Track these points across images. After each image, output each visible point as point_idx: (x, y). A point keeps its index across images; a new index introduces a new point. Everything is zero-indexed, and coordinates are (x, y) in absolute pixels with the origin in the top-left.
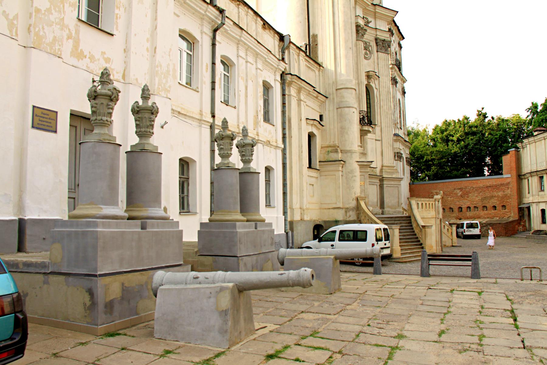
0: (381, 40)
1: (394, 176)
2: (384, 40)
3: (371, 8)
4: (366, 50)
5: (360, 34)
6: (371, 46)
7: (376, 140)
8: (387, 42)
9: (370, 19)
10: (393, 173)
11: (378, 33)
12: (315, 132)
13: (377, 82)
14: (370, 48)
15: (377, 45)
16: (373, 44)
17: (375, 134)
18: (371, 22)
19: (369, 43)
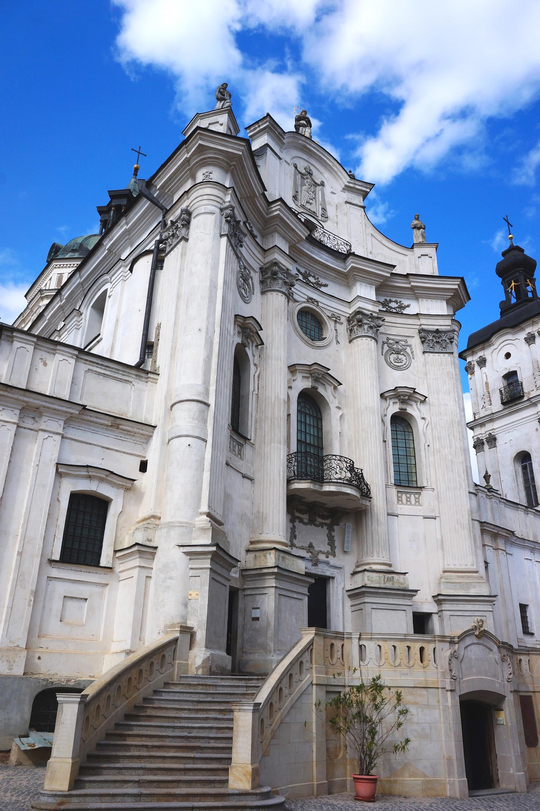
0: (428, 332)
1: (472, 592)
2: (437, 331)
3: (401, 283)
4: (398, 353)
5: (366, 327)
6: (410, 346)
7: (425, 518)
8: (445, 332)
9: (405, 302)
10: (468, 585)
11: (423, 321)
12: (105, 490)
13: (422, 407)
14: (408, 350)
15: (423, 342)
16: (416, 342)
17: (420, 505)
18: (408, 306)
19: (406, 341)
